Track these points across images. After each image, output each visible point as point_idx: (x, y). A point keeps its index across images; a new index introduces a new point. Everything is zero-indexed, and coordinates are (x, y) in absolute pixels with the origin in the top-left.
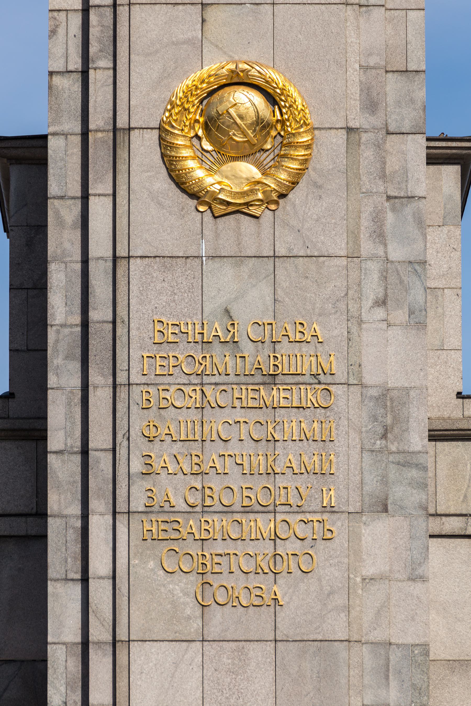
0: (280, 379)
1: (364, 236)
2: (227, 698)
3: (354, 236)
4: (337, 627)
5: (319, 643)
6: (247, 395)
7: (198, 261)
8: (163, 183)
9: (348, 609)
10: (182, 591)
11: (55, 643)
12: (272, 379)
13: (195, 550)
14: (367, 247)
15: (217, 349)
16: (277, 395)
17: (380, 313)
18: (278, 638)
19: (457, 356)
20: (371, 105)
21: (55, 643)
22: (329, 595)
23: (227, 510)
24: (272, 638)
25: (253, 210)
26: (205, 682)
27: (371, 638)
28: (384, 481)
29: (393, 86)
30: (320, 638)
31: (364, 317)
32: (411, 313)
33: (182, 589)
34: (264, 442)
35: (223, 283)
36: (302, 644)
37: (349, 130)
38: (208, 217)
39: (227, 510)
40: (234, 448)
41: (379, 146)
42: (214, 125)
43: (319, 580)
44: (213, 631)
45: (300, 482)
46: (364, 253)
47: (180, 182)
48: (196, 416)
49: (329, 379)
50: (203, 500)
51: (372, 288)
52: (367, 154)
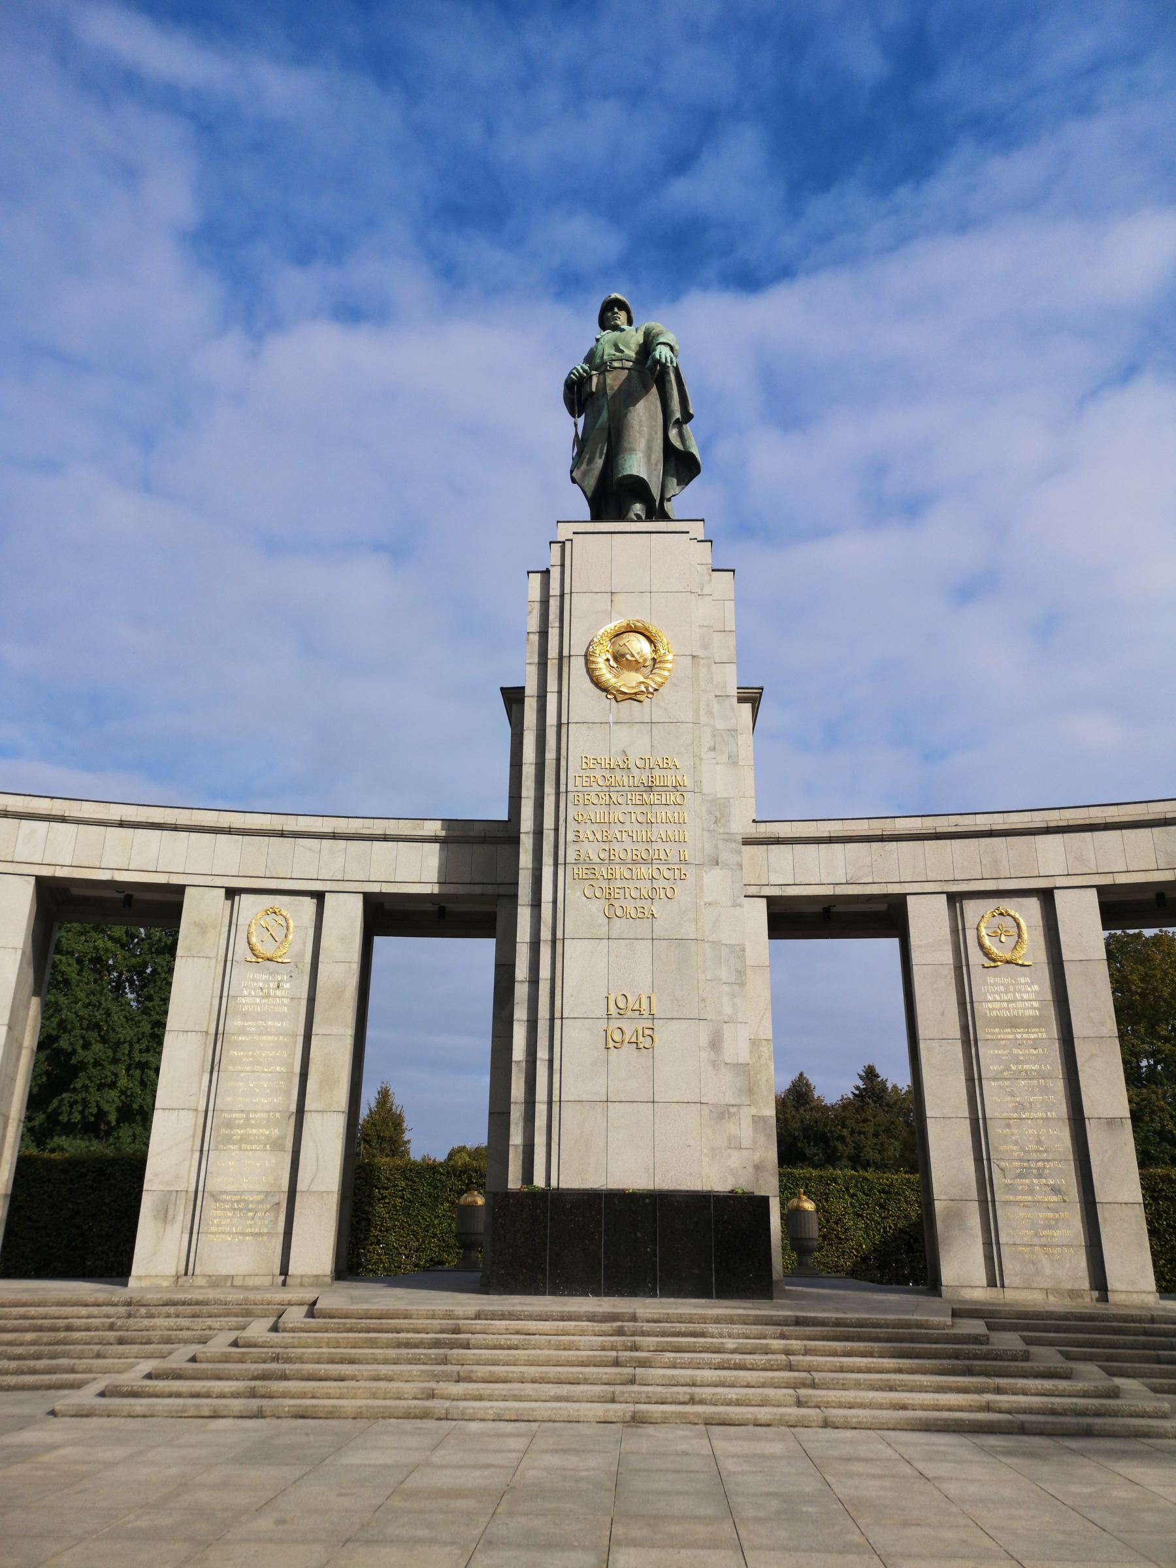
0: (654, 789)
1: (702, 712)
3: (697, 712)
4: (689, 931)
6: (637, 799)
9: (696, 920)
12: (650, 789)
13: (604, 885)
14: (704, 719)
15: (618, 772)
16: (654, 798)
17: (712, 754)
19: (753, 800)
20: (705, 647)
23: (623, 862)
25: (639, 697)
27: (710, 939)
28: (716, 847)
29: (717, 638)
31: (703, 756)
32: (730, 757)
33: (597, 908)
35: (621, 737)
37: (694, 656)
38: (613, 701)
39: (623, 862)
40: (628, 827)
41: (709, 666)
42: (618, 657)
44: (614, 934)
45: (667, 847)
46: (702, 722)
47: (597, 683)
48: (605, 809)
49: (683, 789)
51: (707, 741)
52: (703, 671)
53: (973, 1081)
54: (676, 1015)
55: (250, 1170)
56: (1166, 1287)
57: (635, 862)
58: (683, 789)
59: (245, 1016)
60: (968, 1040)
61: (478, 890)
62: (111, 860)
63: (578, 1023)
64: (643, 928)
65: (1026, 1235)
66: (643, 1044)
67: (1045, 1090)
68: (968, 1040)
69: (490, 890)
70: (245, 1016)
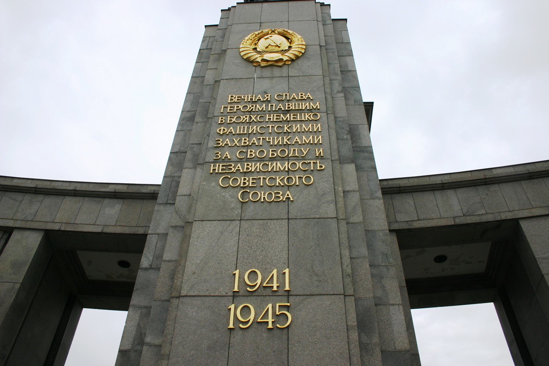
2: (255, 251)
5: (317, 220)
7: (252, 80)
8: (239, 61)
10: (230, 196)
11: (152, 234)
18: (290, 217)
21: (152, 234)
22: (322, 195)
23: (261, 160)
24: (286, 217)
26: (240, 242)
30: (318, 216)
34: (282, 134)
36: (305, 221)
43: (316, 188)
50: (247, 156)
54: (315, 291)
57: (272, 159)
58: (317, 111)
63: (198, 302)
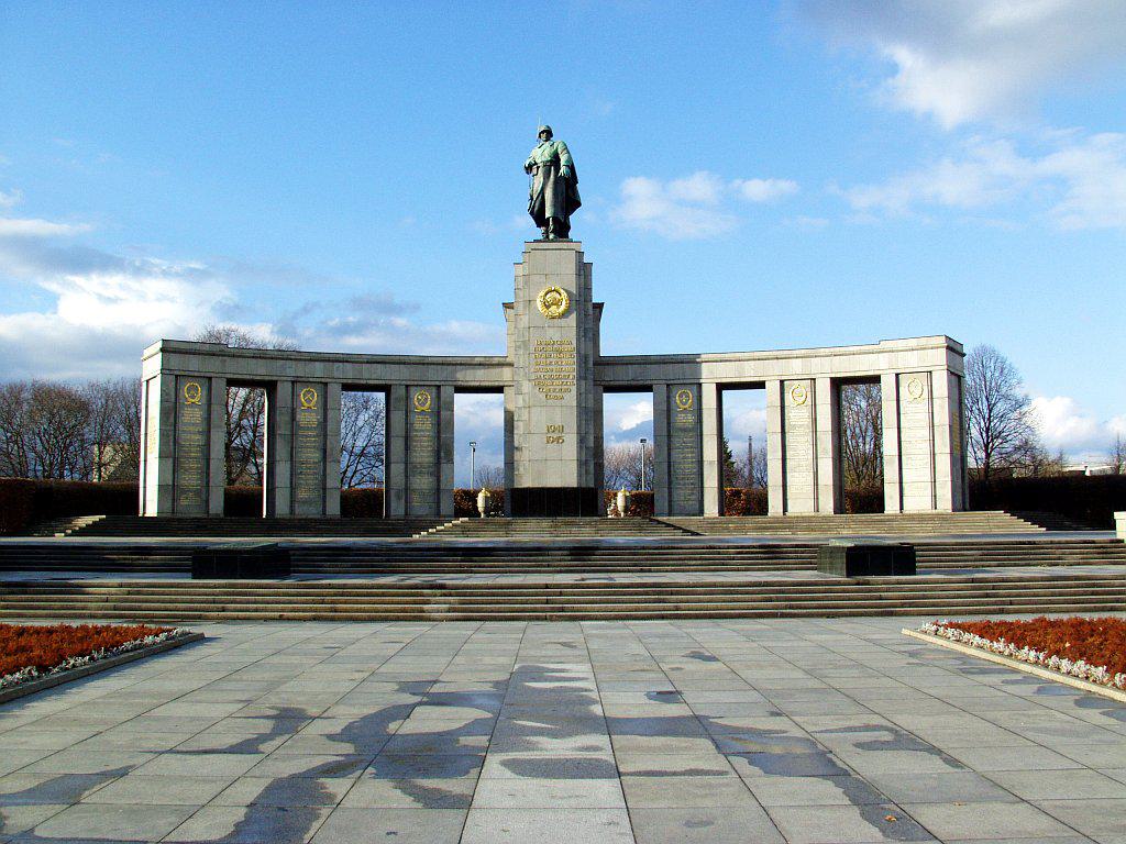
33: (542, 396)
53: (669, 449)
55: (423, 482)
56: (721, 513)
59: (416, 431)
60: (669, 436)
61: (497, 384)
62: (366, 375)
64: (558, 403)
65: (682, 498)
66: (559, 440)
67: (692, 452)
68: (669, 436)
69: (501, 384)
70: (416, 431)
